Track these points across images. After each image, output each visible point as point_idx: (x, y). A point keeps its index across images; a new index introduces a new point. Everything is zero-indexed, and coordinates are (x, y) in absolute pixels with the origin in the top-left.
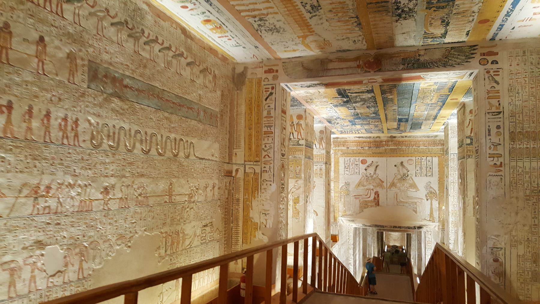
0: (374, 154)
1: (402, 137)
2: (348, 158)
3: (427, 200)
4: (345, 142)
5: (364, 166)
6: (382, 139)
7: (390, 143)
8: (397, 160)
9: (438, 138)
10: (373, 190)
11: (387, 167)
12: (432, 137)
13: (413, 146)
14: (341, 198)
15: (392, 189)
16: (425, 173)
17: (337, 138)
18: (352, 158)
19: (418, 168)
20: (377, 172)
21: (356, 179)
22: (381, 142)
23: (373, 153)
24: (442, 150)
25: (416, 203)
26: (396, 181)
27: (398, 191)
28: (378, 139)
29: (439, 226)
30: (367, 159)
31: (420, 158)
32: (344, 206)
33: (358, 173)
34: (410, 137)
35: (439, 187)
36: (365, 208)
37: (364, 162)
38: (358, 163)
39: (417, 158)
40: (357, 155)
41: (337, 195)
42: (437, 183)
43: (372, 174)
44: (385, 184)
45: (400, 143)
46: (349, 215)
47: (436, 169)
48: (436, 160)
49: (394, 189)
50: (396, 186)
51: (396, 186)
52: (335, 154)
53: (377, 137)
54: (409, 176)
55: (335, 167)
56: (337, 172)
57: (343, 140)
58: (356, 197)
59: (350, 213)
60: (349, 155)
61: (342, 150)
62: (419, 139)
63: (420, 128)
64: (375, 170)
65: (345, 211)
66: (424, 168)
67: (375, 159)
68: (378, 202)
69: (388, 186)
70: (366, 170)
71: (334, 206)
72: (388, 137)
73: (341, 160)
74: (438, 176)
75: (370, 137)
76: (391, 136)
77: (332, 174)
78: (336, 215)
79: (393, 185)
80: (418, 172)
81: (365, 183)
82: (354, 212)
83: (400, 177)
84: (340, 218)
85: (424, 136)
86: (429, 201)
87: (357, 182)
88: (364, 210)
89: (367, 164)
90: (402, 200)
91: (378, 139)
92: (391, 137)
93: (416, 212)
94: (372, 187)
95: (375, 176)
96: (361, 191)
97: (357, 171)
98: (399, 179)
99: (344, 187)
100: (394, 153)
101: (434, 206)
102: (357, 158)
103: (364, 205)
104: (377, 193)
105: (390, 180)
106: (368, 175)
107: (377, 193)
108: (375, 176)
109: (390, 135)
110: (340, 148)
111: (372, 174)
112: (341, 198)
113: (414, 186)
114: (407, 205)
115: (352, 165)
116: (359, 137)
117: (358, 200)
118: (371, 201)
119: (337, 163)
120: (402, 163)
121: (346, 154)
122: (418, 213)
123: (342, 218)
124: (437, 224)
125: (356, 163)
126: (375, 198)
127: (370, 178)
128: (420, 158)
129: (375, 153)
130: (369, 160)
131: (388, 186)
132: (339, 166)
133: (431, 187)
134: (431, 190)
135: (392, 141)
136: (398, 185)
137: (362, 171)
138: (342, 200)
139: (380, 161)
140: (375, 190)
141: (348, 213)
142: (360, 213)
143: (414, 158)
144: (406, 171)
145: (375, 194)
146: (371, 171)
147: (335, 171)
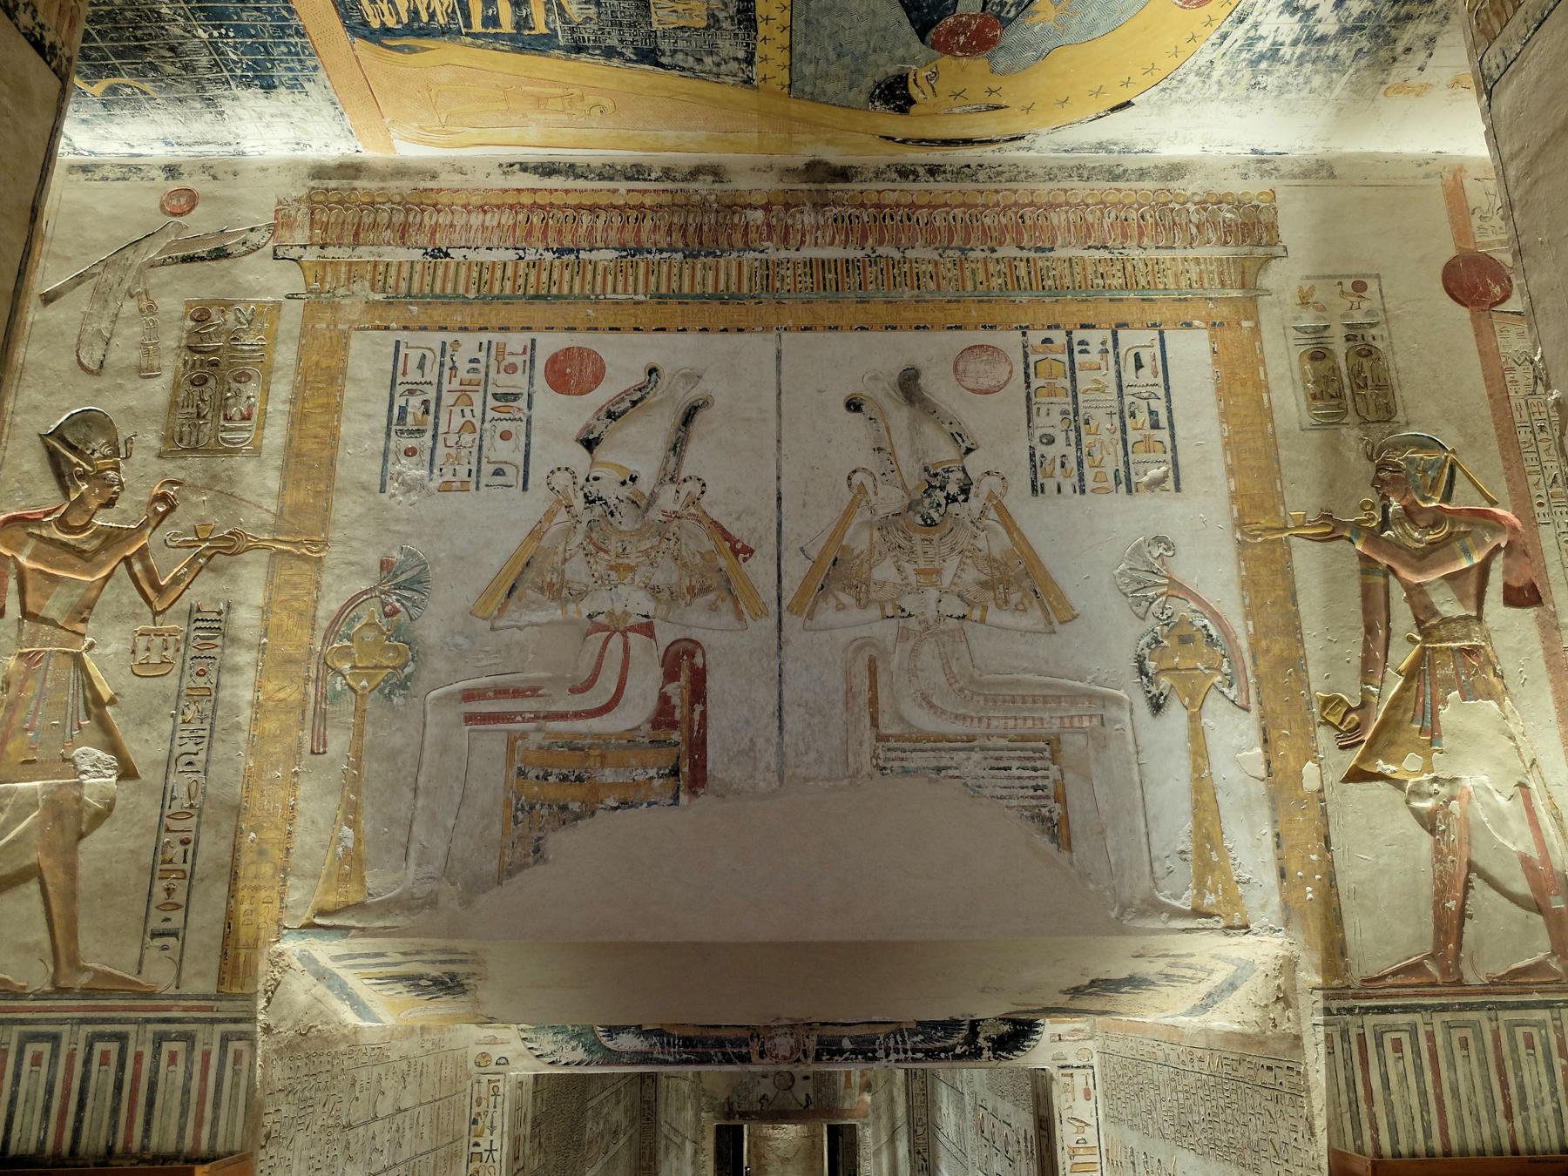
0: (670, 309)
1: (905, 173)
2: (435, 339)
3: (1157, 706)
5: (578, 411)
6: (742, 183)
7: (809, 218)
8: (870, 357)
9: (1190, 187)
10: (647, 629)
11: (782, 416)
12: (1142, 174)
14: (322, 716)
15: (827, 614)
16: (1112, 461)
17: (351, 170)
18: (469, 343)
19: (1052, 421)
20: (697, 458)
21: (499, 524)
22: (732, 206)
23: (661, 298)
24: (1233, 275)
25: (1054, 743)
26: (859, 539)
27: (887, 631)
28: (703, 186)
29: (1289, 966)
30: (608, 347)
32: (352, 814)
33: (513, 476)
35: (1249, 584)
36: (565, 816)
37: (568, 374)
38: (519, 381)
39: (1035, 337)
40: (518, 313)
41: (291, 693)
42: (1229, 550)
43: (645, 485)
44: (759, 570)
46: (386, 908)
47: (1201, 426)
48: (1192, 351)
49: (846, 622)
50: (861, 590)
51: (861, 590)
52: (318, 300)
53: (695, 173)
55: (298, 420)
56: (311, 462)
57: (406, 185)
58: (480, 708)
60: (438, 314)
61: (379, 274)
62: (1044, 189)
64: (677, 448)
65: (353, 863)
66: (1104, 424)
67: (674, 351)
68: (698, 746)
69: (791, 587)
70: (590, 444)
71: (237, 810)
72: (789, 171)
73: (367, 358)
74: (1223, 486)
75: (637, 172)
77: (261, 483)
78: (257, 910)
79: (836, 573)
80: (1052, 452)
81: (577, 571)
82: (447, 873)
83: (890, 499)
84: (291, 946)
86: (1176, 715)
87: (495, 561)
88: (560, 842)
89: (603, 395)
90: (925, 721)
91: (703, 186)
92: (817, 171)
93: (1058, 831)
94: (637, 602)
95: (668, 499)
96: (537, 637)
97: (507, 452)
99: (370, 611)
101: (1223, 770)
102: (516, 342)
103: (556, 791)
104: (685, 665)
105: (809, 528)
106: (610, 490)
107: (685, 665)
108: (668, 499)
110: (365, 253)
112: (322, 716)
113: (1024, 581)
114: (972, 764)
115: (464, 396)
117: (493, 740)
118: (630, 740)
119: (322, 382)
120: (909, 384)
121: (399, 302)
122: (1080, 846)
123: (324, 950)
124: (1263, 948)
125: (504, 383)
126: (663, 716)
127: (627, 520)
128: (1059, 337)
129: (680, 298)
130: (623, 358)
131: (787, 599)
132: (334, 409)
134: (1182, 609)
136: (885, 571)
137: (557, 451)
138: (338, 742)
139: (726, 364)
140: (666, 635)
141: (380, 882)
142: (507, 872)
143: (1009, 340)
144: (946, 452)
145: (671, 675)
146: (638, 449)
147: (293, 458)
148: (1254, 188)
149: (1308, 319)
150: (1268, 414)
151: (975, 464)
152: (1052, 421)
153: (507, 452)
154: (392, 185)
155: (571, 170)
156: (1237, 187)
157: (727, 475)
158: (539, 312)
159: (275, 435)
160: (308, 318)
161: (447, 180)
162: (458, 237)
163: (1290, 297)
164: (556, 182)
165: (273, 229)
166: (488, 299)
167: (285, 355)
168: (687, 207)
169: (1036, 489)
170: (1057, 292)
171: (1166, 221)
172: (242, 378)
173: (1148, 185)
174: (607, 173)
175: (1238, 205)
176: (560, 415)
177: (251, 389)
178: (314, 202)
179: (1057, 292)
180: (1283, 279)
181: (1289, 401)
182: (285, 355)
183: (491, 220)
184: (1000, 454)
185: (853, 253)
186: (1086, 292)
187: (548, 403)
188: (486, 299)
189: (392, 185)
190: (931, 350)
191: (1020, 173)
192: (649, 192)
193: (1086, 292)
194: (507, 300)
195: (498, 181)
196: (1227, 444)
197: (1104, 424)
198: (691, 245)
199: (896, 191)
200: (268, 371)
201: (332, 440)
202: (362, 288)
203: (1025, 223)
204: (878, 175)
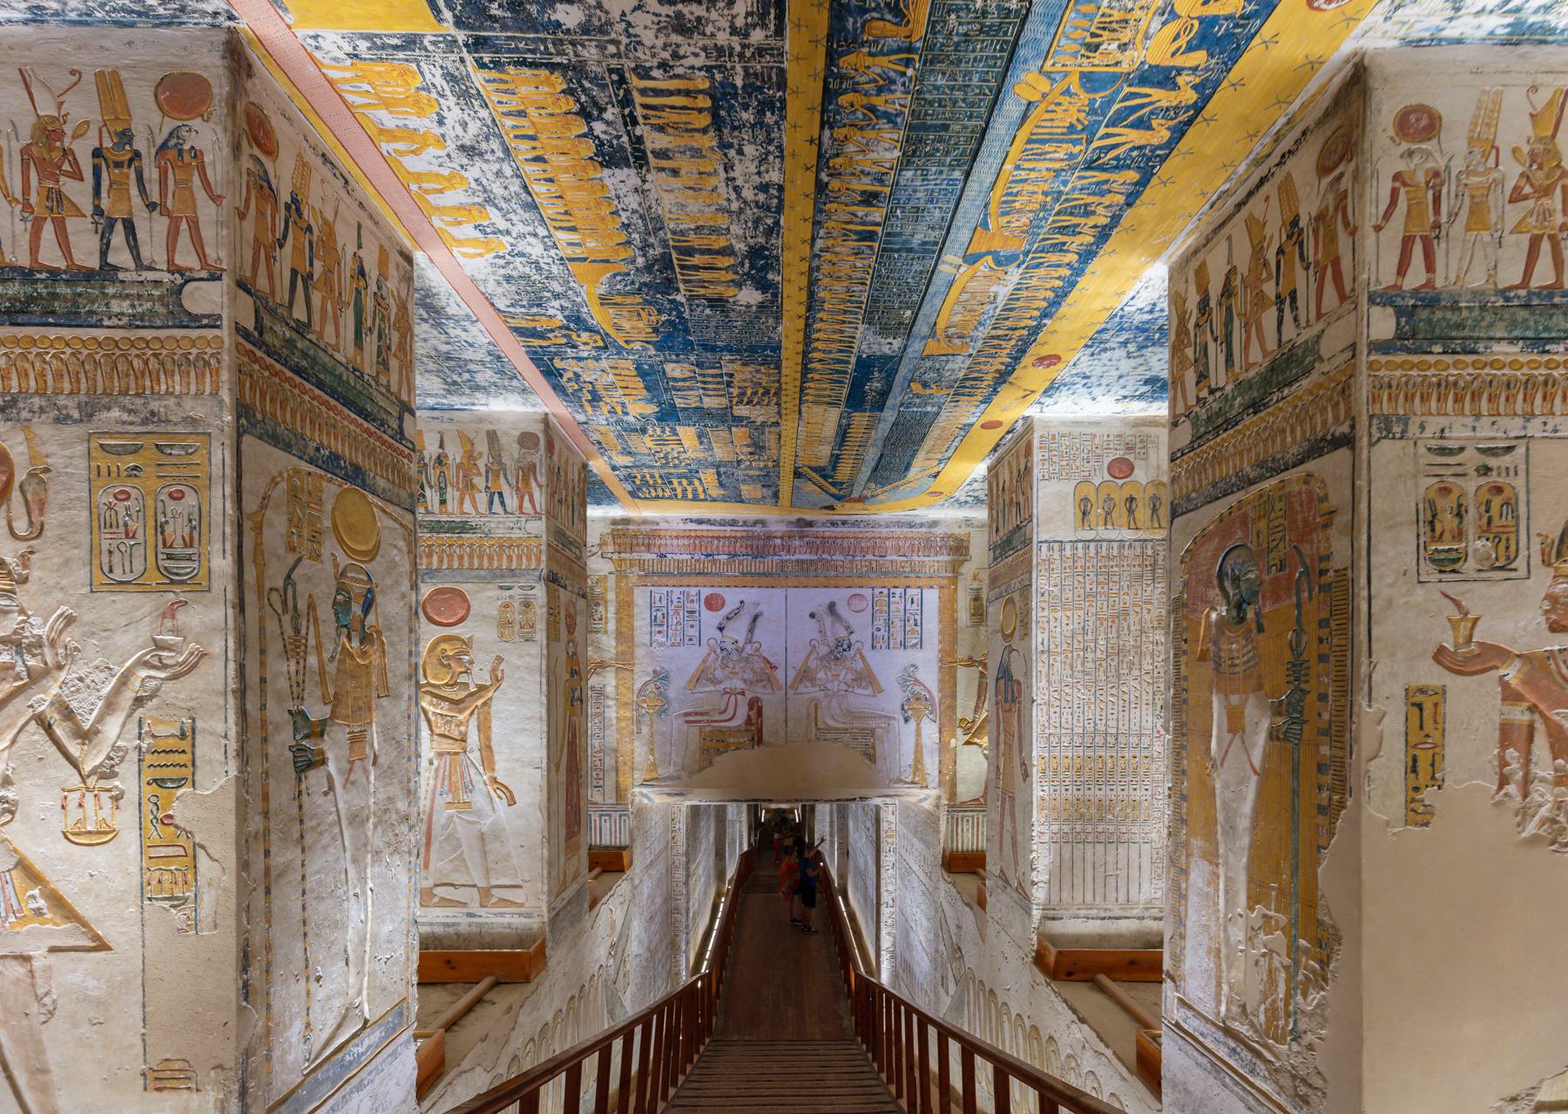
1: (834, 524)
4: (653, 535)
8: (818, 598)
9: (939, 531)
11: (787, 619)
12: (922, 525)
13: (864, 551)
16: (900, 638)
17: (626, 521)
18: (677, 591)
19: (880, 623)
20: (758, 635)
21: (689, 659)
22: (769, 537)
24: (950, 568)
26: (813, 664)
28: (758, 528)
30: (727, 593)
31: (885, 591)
33: (696, 641)
34: (855, 524)
37: (713, 603)
38: (695, 606)
39: (877, 591)
40: (694, 580)
45: (824, 544)
48: (932, 597)
52: (621, 575)
53: (756, 523)
54: (855, 647)
55: (619, 621)
56: (625, 636)
59: (671, 770)
60: (665, 580)
63: (907, 468)
64: (751, 630)
66: (898, 623)
67: (749, 595)
70: (721, 629)
73: (641, 597)
75: (733, 523)
76: (799, 520)
77: (607, 644)
83: (824, 650)
85: (899, 524)
89: (725, 611)
92: (802, 523)
98: (821, 659)
100: (806, 574)
102: (693, 591)
105: (796, 660)
106: (729, 647)
108: (749, 649)
109: (795, 516)
111: (741, 644)
115: (676, 612)
116: (700, 522)
119: (625, 606)
120: (832, 607)
121: (649, 575)
125: (690, 606)
127: (735, 657)
128: (885, 591)
129: (752, 575)
130: (732, 597)
132: (631, 616)
133: (917, 682)
135: (801, 538)
139: (769, 600)
143: (867, 592)
144: (843, 633)
146: (738, 630)
148: (961, 532)
149: (975, 586)
150: (955, 621)
151: (853, 638)
152: (880, 623)
153: (693, 632)
154: (643, 527)
155: (709, 522)
156: (956, 531)
157: (769, 641)
158: (700, 580)
159: (612, 626)
160: (618, 582)
161: (663, 526)
162: (669, 549)
163: (970, 577)
164: (703, 527)
165: (600, 546)
166: (682, 574)
167: (611, 596)
168: (753, 538)
169: (873, 647)
170: (886, 574)
171: (928, 545)
172: (597, 604)
173: (924, 530)
174: (723, 523)
175: (956, 539)
176: (710, 619)
177: (601, 609)
178: (615, 535)
179: (886, 574)
180: (968, 569)
181: (964, 616)
182: (611, 596)
183: (681, 542)
184: (862, 636)
185: (814, 557)
186: (896, 574)
187: (705, 613)
188: (681, 574)
189: (643, 527)
190: (840, 595)
191: (877, 524)
192: (739, 531)
193: (896, 574)
194: (689, 575)
195: (682, 526)
196: (940, 632)
197: (898, 623)
198: (755, 555)
199: (829, 531)
200: (606, 602)
201: (632, 628)
202: (635, 569)
203: (876, 546)
204: (823, 525)
